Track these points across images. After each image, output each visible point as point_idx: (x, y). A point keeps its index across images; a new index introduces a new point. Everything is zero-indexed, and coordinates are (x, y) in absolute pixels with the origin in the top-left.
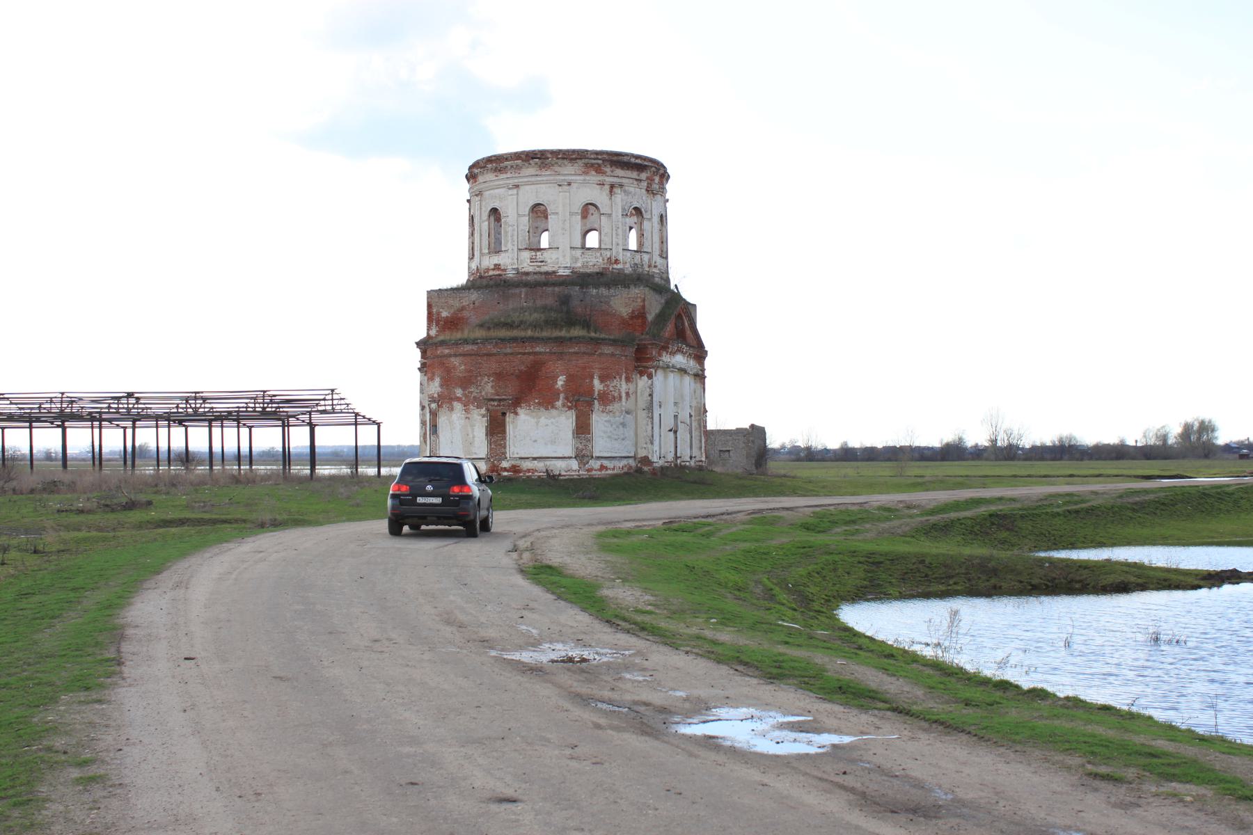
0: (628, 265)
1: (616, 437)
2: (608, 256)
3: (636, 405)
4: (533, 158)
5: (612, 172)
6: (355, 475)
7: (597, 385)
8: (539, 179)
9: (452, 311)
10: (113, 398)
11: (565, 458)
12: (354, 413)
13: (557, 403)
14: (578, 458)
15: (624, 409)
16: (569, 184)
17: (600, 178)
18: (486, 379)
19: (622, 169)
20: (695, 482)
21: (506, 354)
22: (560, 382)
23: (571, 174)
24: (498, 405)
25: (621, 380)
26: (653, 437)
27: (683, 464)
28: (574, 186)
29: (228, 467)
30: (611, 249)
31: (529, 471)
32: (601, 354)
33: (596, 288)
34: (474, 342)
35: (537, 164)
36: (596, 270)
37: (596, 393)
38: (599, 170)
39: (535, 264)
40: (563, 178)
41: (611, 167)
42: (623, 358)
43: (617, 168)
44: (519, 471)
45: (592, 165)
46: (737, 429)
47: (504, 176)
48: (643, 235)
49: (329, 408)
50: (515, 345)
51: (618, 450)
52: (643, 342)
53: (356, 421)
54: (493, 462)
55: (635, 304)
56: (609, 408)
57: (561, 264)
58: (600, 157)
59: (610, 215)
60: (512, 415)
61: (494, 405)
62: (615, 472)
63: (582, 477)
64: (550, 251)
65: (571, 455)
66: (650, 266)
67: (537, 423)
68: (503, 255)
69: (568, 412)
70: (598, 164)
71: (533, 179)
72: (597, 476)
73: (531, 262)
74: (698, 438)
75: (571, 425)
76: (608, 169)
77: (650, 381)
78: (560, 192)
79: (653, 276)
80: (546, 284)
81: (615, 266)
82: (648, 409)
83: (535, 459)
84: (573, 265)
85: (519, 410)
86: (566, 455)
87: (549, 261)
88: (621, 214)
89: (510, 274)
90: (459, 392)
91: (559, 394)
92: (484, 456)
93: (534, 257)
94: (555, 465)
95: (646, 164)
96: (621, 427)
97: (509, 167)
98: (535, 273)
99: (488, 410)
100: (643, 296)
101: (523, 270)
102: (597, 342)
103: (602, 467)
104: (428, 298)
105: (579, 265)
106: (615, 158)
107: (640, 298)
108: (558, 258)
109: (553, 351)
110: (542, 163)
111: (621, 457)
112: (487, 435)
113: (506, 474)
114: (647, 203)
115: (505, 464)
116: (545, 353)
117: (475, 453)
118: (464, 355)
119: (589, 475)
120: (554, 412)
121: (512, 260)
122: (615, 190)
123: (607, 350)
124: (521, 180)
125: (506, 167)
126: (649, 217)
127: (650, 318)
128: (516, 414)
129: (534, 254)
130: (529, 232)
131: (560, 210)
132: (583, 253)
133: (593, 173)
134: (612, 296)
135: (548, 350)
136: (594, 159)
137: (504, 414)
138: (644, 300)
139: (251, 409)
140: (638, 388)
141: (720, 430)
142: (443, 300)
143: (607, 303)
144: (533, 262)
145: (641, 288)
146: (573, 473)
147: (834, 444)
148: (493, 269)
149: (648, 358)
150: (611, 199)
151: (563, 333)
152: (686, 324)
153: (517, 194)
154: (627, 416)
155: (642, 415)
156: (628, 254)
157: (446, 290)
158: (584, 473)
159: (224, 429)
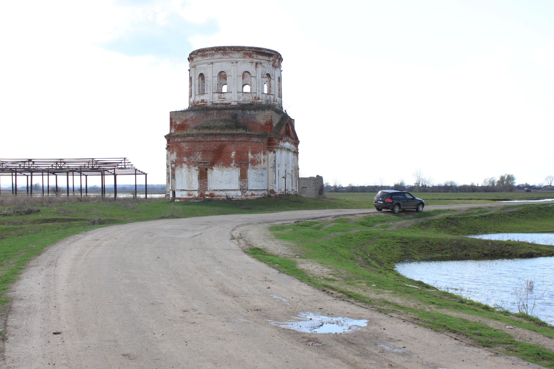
0: (264, 101)
1: (259, 180)
2: (255, 96)
3: (268, 165)
4: (220, 50)
5: (257, 57)
6: (135, 198)
7: (250, 156)
8: (223, 60)
9: (182, 121)
10: (22, 162)
11: (235, 190)
12: (135, 169)
13: (231, 164)
14: (241, 190)
15: (262, 167)
16: (237, 62)
17: (251, 59)
18: (198, 153)
19: (261, 55)
20: (295, 202)
21: (208, 141)
22: (233, 154)
23: (238, 58)
24: (204, 165)
25: (261, 154)
26: (276, 180)
27: (289, 193)
28: (239, 63)
29: (76, 194)
30: (256, 93)
31: (218, 196)
32: (252, 142)
33: (249, 111)
34: (193, 135)
35: (221, 53)
36: (249, 102)
37: (250, 160)
38: (250, 56)
39: (221, 99)
40: (234, 59)
41: (256, 55)
42: (262, 143)
43: (259, 55)
44: (214, 196)
45: (247, 54)
46: (310, 177)
47: (206, 58)
48: (271, 86)
49: (123, 167)
50: (212, 137)
51: (260, 186)
52: (271, 136)
53: (136, 173)
54: (201, 192)
55: (267, 118)
56: (256, 167)
57: (233, 100)
58: (251, 50)
59: (256, 77)
60: (210, 170)
61: (202, 165)
62: (258, 196)
63: (243, 199)
64: (228, 93)
65: (238, 189)
66: (274, 101)
67: (222, 174)
68: (205, 95)
69: (237, 169)
70: (250, 53)
71: (220, 60)
72: (250, 199)
73: (219, 99)
74: (295, 181)
75: (238, 175)
76: (255, 56)
77: (274, 155)
78: (232, 66)
79: (275, 106)
80: (226, 109)
81: (258, 101)
82: (274, 167)
83: (221, 190)
84: (238, 100)
85: (214, 168)
86: (235, 189)
87: (227, 98)
88: (261, 76)
89: (209, 104)
90: (185, 159)
91: (232, 160)
92: (197, 189)
93: (220, 96)
94: (230, 193)
95: (272, 53)
96: (261, 176)
97: (209, 54)
98: (221, 104)
99: (199, 167)
100: (271, 115)
101: (215, 102)
102: (250, 136)
103: (252, 195)
104: (170, 115)
105: (241, 100)
106: (258, 51)
107: (270, 115)
108: (231, 97)
109: (230, 140)
110: (224, 52)
112: (198, 179)
113: (207, 197)
114: (273, 72)
115: (207, 193)
116: (226, 141)
117: (193, 188)
118: (188, 142)
119: (247, 198)
120: (230, 168)
121: (210, 98)
122: (258, 65)
123: (255, 140)
124: (214, 60)
125: (207, 54)
126: (273, 78)
127: (274, 125)
128: (212, 169)
129: (220, 95)
130: (218, 84)
131: (232, 74)
132: (243, 95)
133: (248, 57)
134: (257, 115)
135: (227, 140)
136: (249, 51)
137: (206, 169)
138: (272, 117)
139: (87, 167)
140: (269, 158)
141: (302, 178)
142: (177, 116)
143: (255, 118)
144: (220, 99)
145: (270, 111)
146: (239, 197)
147: (345, 185)
148: (201, 102)
149: (273, 143)
150: (256, 69)
151: (234, 132)
153: (212, 67)
154: (264, 170)
155: (271, 170)
156: (264, 95)
157: (179, 111)
158: (245, 197)
159: (74, 176)
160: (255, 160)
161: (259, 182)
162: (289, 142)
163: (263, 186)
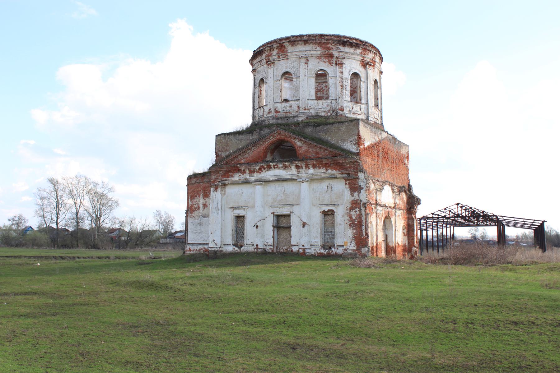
42: (201, 184)
96: (198, 225)
111: (197, 244)
152: (299, 144)
154: (203, 218)
160: (193, 207)
161: (195, 233)
162: (276, 167)
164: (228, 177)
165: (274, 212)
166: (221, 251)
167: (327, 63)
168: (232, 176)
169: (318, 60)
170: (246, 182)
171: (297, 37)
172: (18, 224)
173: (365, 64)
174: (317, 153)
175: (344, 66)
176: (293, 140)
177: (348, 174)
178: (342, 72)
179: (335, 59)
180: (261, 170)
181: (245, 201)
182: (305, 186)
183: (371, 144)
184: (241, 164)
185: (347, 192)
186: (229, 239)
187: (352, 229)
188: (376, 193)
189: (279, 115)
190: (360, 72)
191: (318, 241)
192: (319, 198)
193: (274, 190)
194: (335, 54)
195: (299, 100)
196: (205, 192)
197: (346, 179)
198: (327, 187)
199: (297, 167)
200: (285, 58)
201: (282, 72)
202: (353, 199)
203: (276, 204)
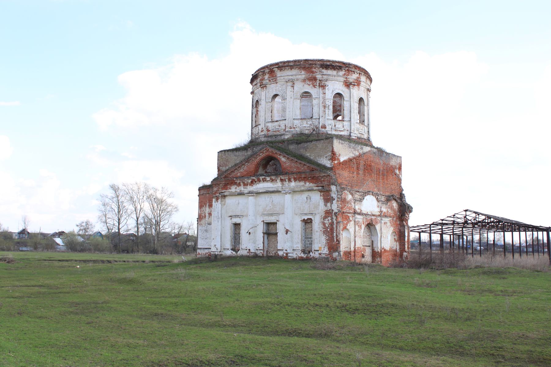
25: (206, 207)
42: (207, 195)
51: (204, 244)
96: (205, 232)
111: (203, 248)
152: (283, 159)
161: (203, 239)
162: (264, 180)
163: (207, 243)
164: (227, 190)
165: (264, 220)
166: (221, 255)
167: (311, 85)
168: (230, 189)
169: (303, 83)
170: (241, 194)
171: (284, 62)
172: (85, 230)
173: (348, 85)
174: (298, 168)
175: (327, 88)
176: (279, 156)
177: (323, 186)
178: (325, 93)
179: (318, 82)
180: (252, 183)
181: (241, 210)
182: (288, 197)
183: (349, 158)
184: (237, 178)
185: (322, 203)
186: (228, 244)
187: (325, 235)
188: (355, 203)
189: (270, 133)
190: (343, 92)
191: (299, 246)
192: (300, 208)
193: (264, 200)
194: (319, 77)
195: (286, 120)
196: (210, 202)
197: (321, 191)
198: (307, 198)
199: (281, 180)
200: (275, 82)
201: (272, 95)
202: (326, 209)
203: (265, 213)
